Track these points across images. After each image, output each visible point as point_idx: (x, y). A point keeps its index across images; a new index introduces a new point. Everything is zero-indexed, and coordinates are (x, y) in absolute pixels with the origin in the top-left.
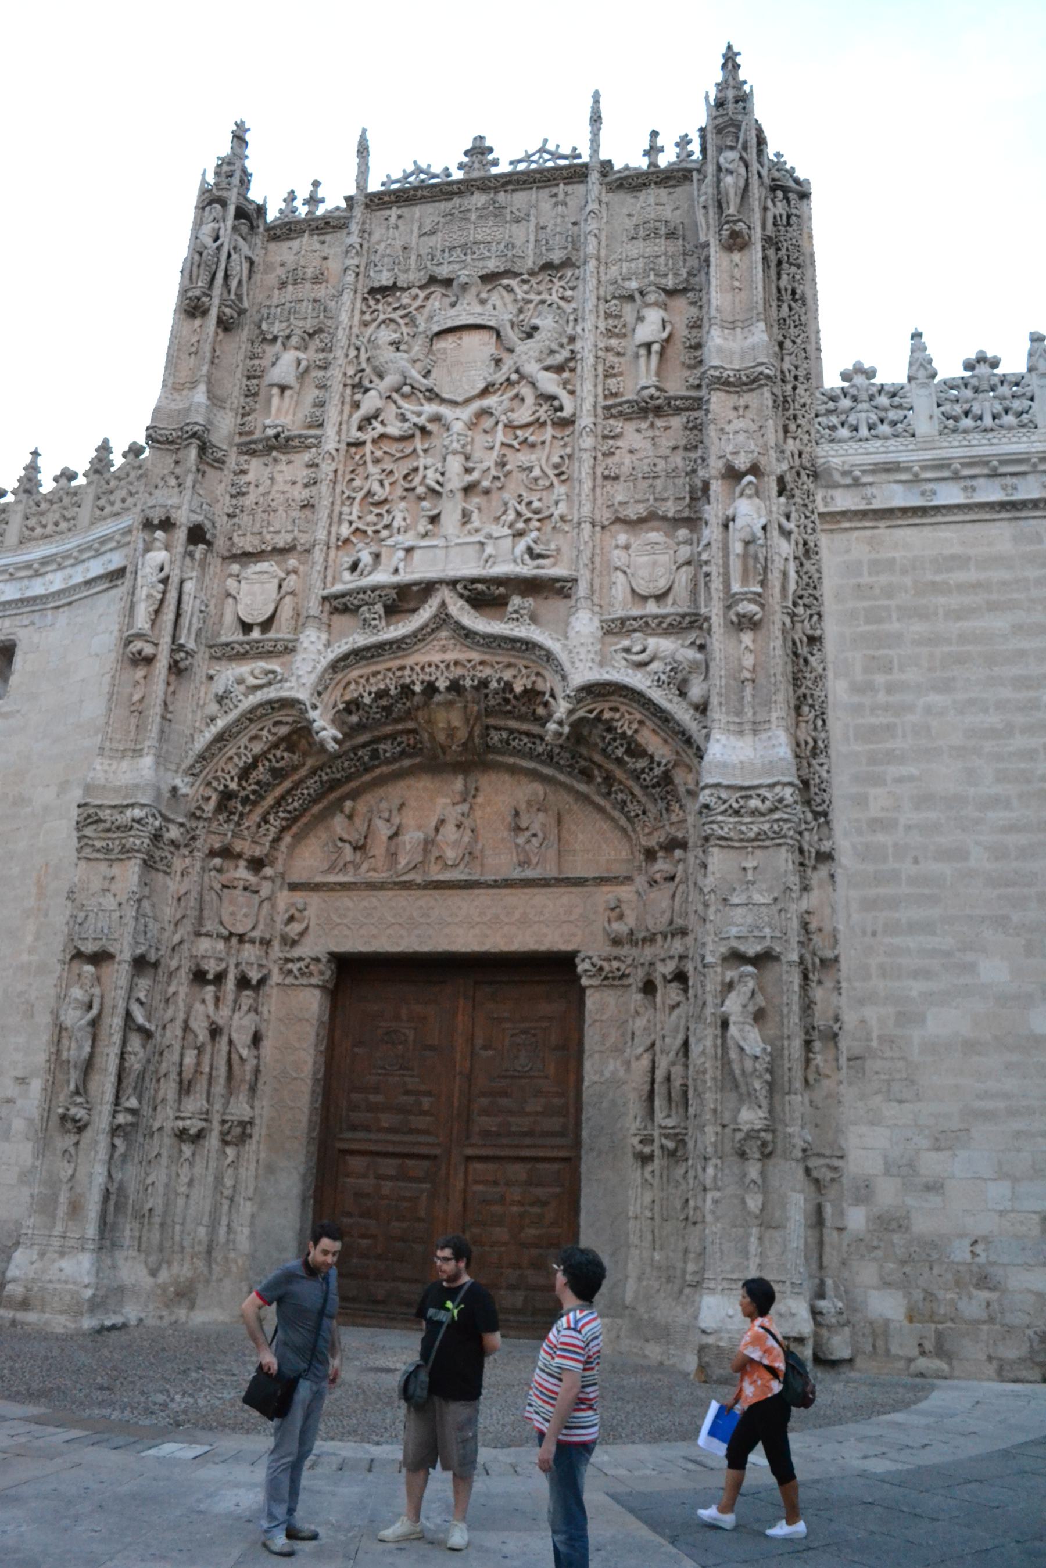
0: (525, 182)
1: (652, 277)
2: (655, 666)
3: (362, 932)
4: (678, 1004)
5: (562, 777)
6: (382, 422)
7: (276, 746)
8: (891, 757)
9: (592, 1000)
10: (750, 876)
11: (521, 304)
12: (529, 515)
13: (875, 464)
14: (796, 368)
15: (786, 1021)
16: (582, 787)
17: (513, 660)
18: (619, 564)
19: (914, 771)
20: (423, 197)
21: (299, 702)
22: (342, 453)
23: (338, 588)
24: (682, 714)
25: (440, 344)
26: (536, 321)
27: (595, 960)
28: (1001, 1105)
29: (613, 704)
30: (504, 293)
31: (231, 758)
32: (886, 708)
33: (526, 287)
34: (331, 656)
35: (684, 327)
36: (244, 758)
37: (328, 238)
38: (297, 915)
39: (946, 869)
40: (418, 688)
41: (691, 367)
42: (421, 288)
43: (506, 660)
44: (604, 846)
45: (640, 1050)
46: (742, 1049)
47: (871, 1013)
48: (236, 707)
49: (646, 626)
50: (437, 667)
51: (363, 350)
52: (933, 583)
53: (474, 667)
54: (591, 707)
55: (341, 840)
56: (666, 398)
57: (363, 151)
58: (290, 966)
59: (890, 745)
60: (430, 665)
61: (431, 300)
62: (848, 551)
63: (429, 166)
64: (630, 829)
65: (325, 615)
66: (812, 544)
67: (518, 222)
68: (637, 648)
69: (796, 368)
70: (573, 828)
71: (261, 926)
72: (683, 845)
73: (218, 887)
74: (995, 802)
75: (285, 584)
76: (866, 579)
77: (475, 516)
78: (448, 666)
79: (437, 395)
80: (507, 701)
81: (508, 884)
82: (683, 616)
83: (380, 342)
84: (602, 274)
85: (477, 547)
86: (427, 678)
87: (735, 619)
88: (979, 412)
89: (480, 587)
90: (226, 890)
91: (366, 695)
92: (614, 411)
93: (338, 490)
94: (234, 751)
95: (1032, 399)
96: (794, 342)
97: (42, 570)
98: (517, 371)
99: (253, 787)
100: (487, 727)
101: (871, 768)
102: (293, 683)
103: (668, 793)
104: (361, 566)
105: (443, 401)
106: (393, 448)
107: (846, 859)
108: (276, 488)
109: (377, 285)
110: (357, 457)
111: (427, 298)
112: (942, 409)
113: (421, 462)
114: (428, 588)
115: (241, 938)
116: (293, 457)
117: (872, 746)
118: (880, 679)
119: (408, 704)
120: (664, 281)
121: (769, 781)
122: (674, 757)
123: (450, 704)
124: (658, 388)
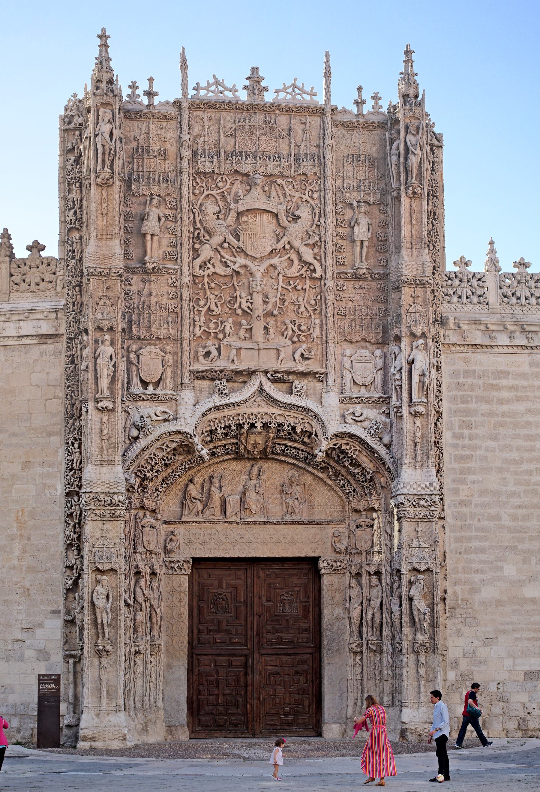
3: (209, 546)
4: (377, 586)
5: (310, 469)
6: (213, 265)
8: (470, 471)
9: (326, 581)
10: (420, 535)
11: (288, 198)
12: (300, 333)
16: (320, 475)
17: (295, 415)
19: (481, 479)
22: (192, 282)
23: (197, 367)
24: (382, 451)
25: (244, 219)
27: (329, 561)
28: (510, 627)
29: (346, 442)
32: (469, 447)
34: (203, 408)
36: (154, 460)
38: (174, 538)
39: (492, 524)
40: (246, 426)
43: (292, 414)
45: (356, 605)
46: (418, 610)
47: (458, 588)
49: (361, 401)
50: (256, 416)
52: (492, 385)
59: (469, 465)
62: (453, 365)
64: (344, 497)
70: (313, 494)
71: (159, 546)
73: (141, 527)
74: (513, 494)
75: (166, 360)
76: (461, 380)
81: (284, 523)
82: (380, 398)
85: (275, 351)
86: (251, 421)
89: (279, 375)
91: (218, 428)
93: (191, 306)
94: (148, 456)
98: (289, 243)
99: (156, 474)
102: (181, 422)
104: (212, 356)
105: (247, 255)
107: (449, 519)
110: (200, 286)
112: (502, 291)
113: (238, 293)
114: (251, 373)
115: (151, 552)
118: (466, 432)
120: (366, 198)
121: (430, 493)
122: (376, 470)
123: (260, 433)
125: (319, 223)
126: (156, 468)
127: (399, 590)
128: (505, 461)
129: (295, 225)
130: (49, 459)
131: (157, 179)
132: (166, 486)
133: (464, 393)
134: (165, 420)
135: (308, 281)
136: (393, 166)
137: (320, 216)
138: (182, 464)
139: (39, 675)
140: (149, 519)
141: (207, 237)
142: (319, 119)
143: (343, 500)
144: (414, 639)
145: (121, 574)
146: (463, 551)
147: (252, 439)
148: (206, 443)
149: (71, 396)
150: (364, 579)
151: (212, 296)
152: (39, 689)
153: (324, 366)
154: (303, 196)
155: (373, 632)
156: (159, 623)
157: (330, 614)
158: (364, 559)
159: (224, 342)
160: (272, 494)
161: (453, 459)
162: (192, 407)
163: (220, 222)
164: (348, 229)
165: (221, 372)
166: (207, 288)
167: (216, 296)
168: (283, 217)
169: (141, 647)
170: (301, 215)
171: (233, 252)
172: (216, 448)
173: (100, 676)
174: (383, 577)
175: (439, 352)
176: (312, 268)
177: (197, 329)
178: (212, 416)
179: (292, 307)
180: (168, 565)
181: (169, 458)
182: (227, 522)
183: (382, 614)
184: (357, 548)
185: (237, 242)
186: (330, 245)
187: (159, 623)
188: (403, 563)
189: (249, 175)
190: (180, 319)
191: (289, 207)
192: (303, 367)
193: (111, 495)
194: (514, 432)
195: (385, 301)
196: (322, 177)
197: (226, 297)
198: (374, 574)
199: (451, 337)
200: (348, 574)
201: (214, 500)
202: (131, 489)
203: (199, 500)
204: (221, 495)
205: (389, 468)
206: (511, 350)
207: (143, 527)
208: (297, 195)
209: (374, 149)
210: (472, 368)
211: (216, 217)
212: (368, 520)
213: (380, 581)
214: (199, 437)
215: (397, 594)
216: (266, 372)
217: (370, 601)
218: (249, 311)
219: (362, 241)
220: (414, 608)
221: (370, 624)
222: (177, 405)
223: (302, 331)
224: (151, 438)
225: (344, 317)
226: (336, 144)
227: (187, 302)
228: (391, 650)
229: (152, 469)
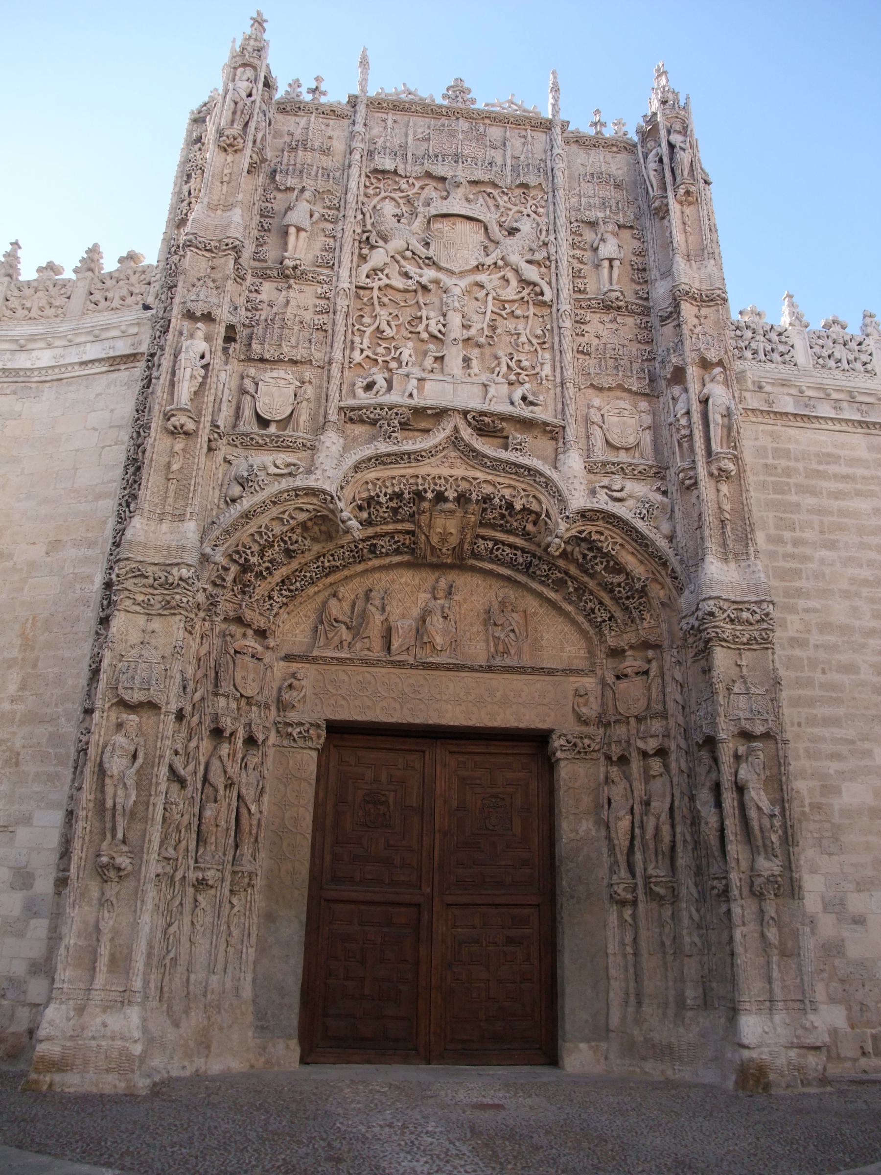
0: (500, 121)
1: (608, 212)
2: (631, 503)
3: (357, 703)
6: (387, 275)
7: (292, 530)
8: (799, 593)
13: (774, 379)
15: (785, 787)
17: (513, 483)
18: (596, 420)
19: (818, 606)
20: (417, 112)
21: (324, 492)
22: (353, 294)
23: (351, 402)
25: (437, 225)
26: (515, 225)
29: (598, 529)
30: (488, 198)
31: (252, 535)
32: (793, 556)
33: (506, 198)
36: (265, 537)
37: (331, 122)
38: (296, 683)
40: (429, 495)
41: (639, 283)
42: (415, 178)
43: (507, 482)
44: (566, 646)
46: (759, 808)
49: (622, 470)
51: (368, 216)
52: (818, 471)
54: (582, 528)
55: (336, 621)
56: (626, 302)
57: (364, 63)
60: (440, 478)
62: (756, 439)
65: (342, 422)
71: (266, 692)
72: (657, 647)
73: (232, 652)
76: (770, 461)
77: (475, 363)
79: (434, 263)
82: (651, 467)
83: (385, 213)
85: (481, 387)
86: (437, 488)
88: (839, 357)
90: (238, 655)
91: (382, 495)
92: (584, 304)
93: (350, 322)
94: (255, 529)
95: (870, 355)
97: (29, 347)
98: (502, 259)
99: (267, 564)
100: (478, 536)
101: (786, 600)
103: (640, 604)
104: (377, 387)
105: (440, 268)
106: (398, 297)
108: (289, 310)
109: (380, 167)
110: (365, 300)
111: (422, 188)
112: (814, 350)
113: (424, 313)
114: (441, 413)
116: (306, 288)
118: (787, 535)
119: (414, 508)
122: (651, 576)
123: (452, 512)
127: (714, 775)
128: (853, 581)
130: (89, 535)
131: (313, 173)
132: (287, 593)
133: (778, 479)
134: (290, 474)
135: (531, 306)
136: (652, 173)
140: (251, 643)
141: (381, 243)
142: (544, 135)
144: (752, 869)
145: (167, 714)
149: (138, 433)
150: (636, 765)
154: (523, 209)
155: (657, 861)
156: (254, 832)
157: (572, 831)
160: (472, 625)
165: (390, 409)
167: (390, 314)
168: (494, 228)
170: (521, 227)
172: (377, 536)
173: (97, 922)
174: (673, 757)
176: (537, 289)
179: (508, 338)
180: (283, 729)
181: (294, 537)
182: (392, 662)
183: (673, 826)
185: (426, 251)
187: (254, 832)
188: (721, 720)
190: (330, 338)
191: (503, 219)
192: (526, 412)
193: (168, 568)
194: (860, 539)
195: (650, 342)
196: (550, 190)
197: (406, 315)
198: (655, 755)
199: (749, 401)
200: (602, 759)
201: (371, 625)
203: (345, 623)
204: (382, 618)
206: (838, 427)
207: (236, 652)
209: (620, 172)
213: (666, 766)
215: (708, 784)
216: (465, 413)
217: (647, 804)
220: (749, 804)
221: (651, 845)
223: (522, 369)
225: (587, 357)
227: (343, 315)
228: (696, 895)
229: (262, 554)
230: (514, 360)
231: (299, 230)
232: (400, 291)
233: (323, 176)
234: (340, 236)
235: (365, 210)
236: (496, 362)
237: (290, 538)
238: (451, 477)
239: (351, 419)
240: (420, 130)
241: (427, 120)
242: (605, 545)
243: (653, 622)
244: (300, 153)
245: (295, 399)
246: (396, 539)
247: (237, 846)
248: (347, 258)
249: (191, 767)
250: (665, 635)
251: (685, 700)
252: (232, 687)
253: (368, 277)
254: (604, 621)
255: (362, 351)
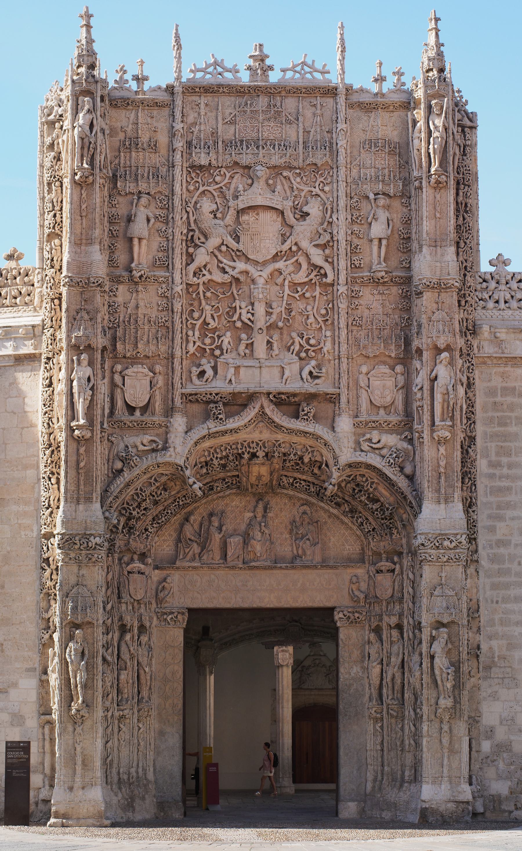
5: (322, 504)
6: (209, 271)
8: (509, 506)
11: (296, 192)
12: (309, 348)
14: (466, 261)
22: (185, 291)
25: (244, 218)
30: (284, 182)
32: (508, 477)
35: (399, 222)
37: (155, 113)
40: (246, 456)
42: (227, 167)
47: (494, 643)
48: (136, 466)
50: (258, 444)
53: (279, 445)
58: (165, 617)
59: (508, 499)
61: (234, 180)
63: (222, 60)
66: (472, 379)
67: (290, 124)
68: (374, 441)
69: (466, 261)
73: (126, 573)
76: (499, 399)
78: (264, 444)
80: (298, 464)
83: (204, 211)
84: (348, 177)
85: (279, 369)
86: (251, 450)
87: (437, 438)
89: (283, 397)
90: (130, 575)
91: (214, 459)
94: (133, 491)
96: (465, 243)
98: (296, 244)
99: (143, 512)
101: (498, 512)
103: (390, 523)
104: (206, 376)
107: (484, 562)
113: (237, 303)
117: (499, 499)
118: (505, 460)
119: (237, 463)
120: (386, 189)
124: (386, 272)
125: (331, 220)
126: (144, 505)
129: (302, 223)
133: (502, 414)
134: (154, 450)
137: (332, 212)
138: (175, 500)
139: (7, 743)
141: (203, 239)
143: (362, 541)
146: (500, 600)
147: (255, 470)
148: (202, 476)
151: (208, 308)
152: (7, 758)
153: (336, 385)
154: (313, 189)
158: (384, 609)
159: (221, 360)
161: (488, 492)
162: (183, 435)
163: (217, 221)
164: (366, 226)
166: (202, 297)
167: (213, 306)
169: (126, 712)
170: (310, 211)
171: (232, 256)
175: (472, 367)
176: (322, 272)
177: (191, 344)
178: (207, 444)
184: (376, 597)
185: (236, 244)
186: (343, 244)
189: (251, 167)
190: (171, 333)
191: (296, 203)
196: (335, 166)
197: (224, 307)
199: (486, 349)
202: (114, 530)
205: (410, 502)
207: (129, 572)
208: (306, 189)
209: (395, 133)
210: (510, 384)
211: (212, 216)
212: (388, 564)
214: (192, 470)
216: (269, 394)
218: (250, 323)
219: (380, 240)
222: (167, 433)
223: (311, 346)
224: (136, 471)
225: (360, 328)
226: (352, 129)
227: (179, 314)
229: (139, 506)
230: (304, 339)
231: (140, 239)
232: (218, 283)
233: (153, 178)
234: (171, 238)
235: (188, 209)
236: (291, 341)
237: (156, 493)
238: (260, 441)
239: (190, 401)
240: (227, 112)
241: (233, 99)
242: (365, 485)
243: (398, 536)
244: (133, 154)
245: (151, 388)
246: (227, 480)
247: (139, 692)
248: (178, 262)
249: (110, 650)
250: (405, 546)
251: (414, 592)
252: (128, 596)
253: (195, 274)
254: (370, 531)
255: (194, 342)
